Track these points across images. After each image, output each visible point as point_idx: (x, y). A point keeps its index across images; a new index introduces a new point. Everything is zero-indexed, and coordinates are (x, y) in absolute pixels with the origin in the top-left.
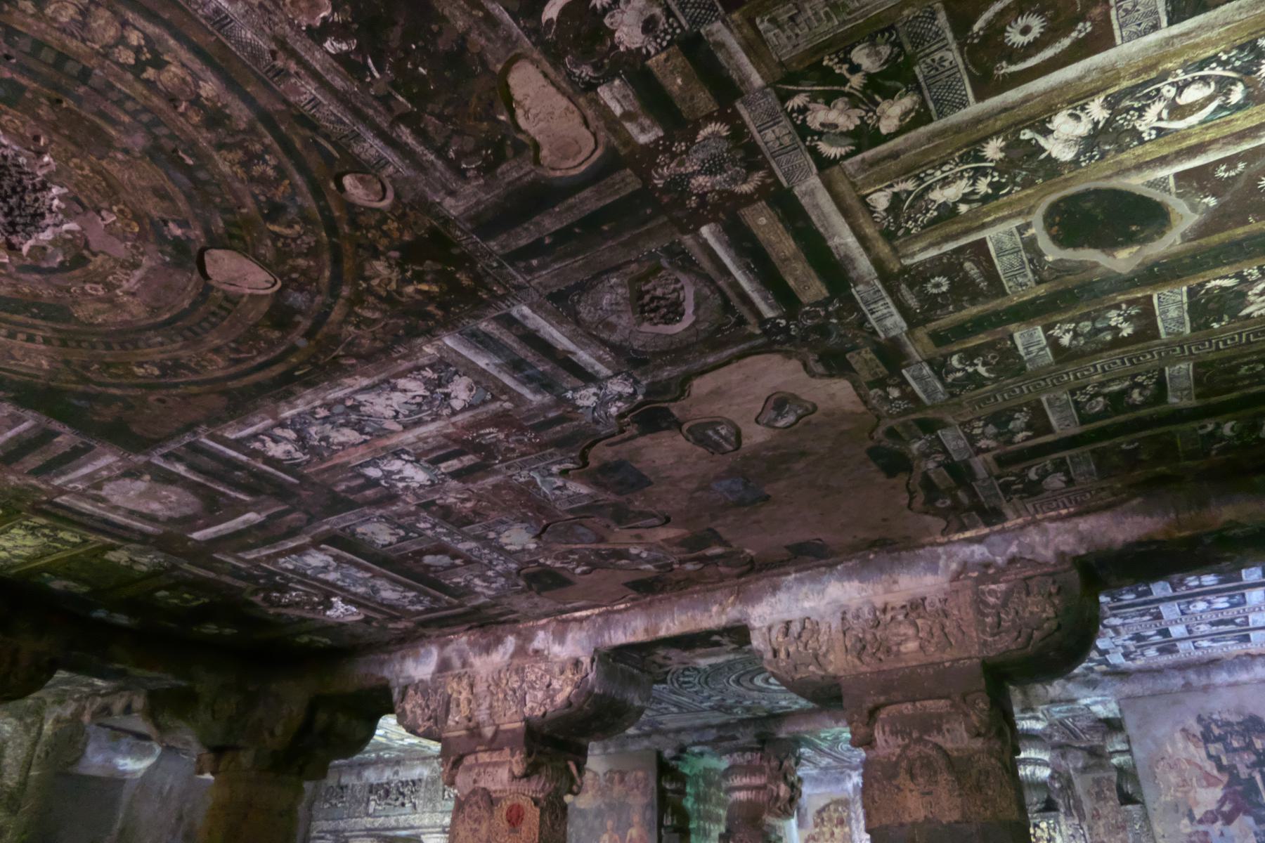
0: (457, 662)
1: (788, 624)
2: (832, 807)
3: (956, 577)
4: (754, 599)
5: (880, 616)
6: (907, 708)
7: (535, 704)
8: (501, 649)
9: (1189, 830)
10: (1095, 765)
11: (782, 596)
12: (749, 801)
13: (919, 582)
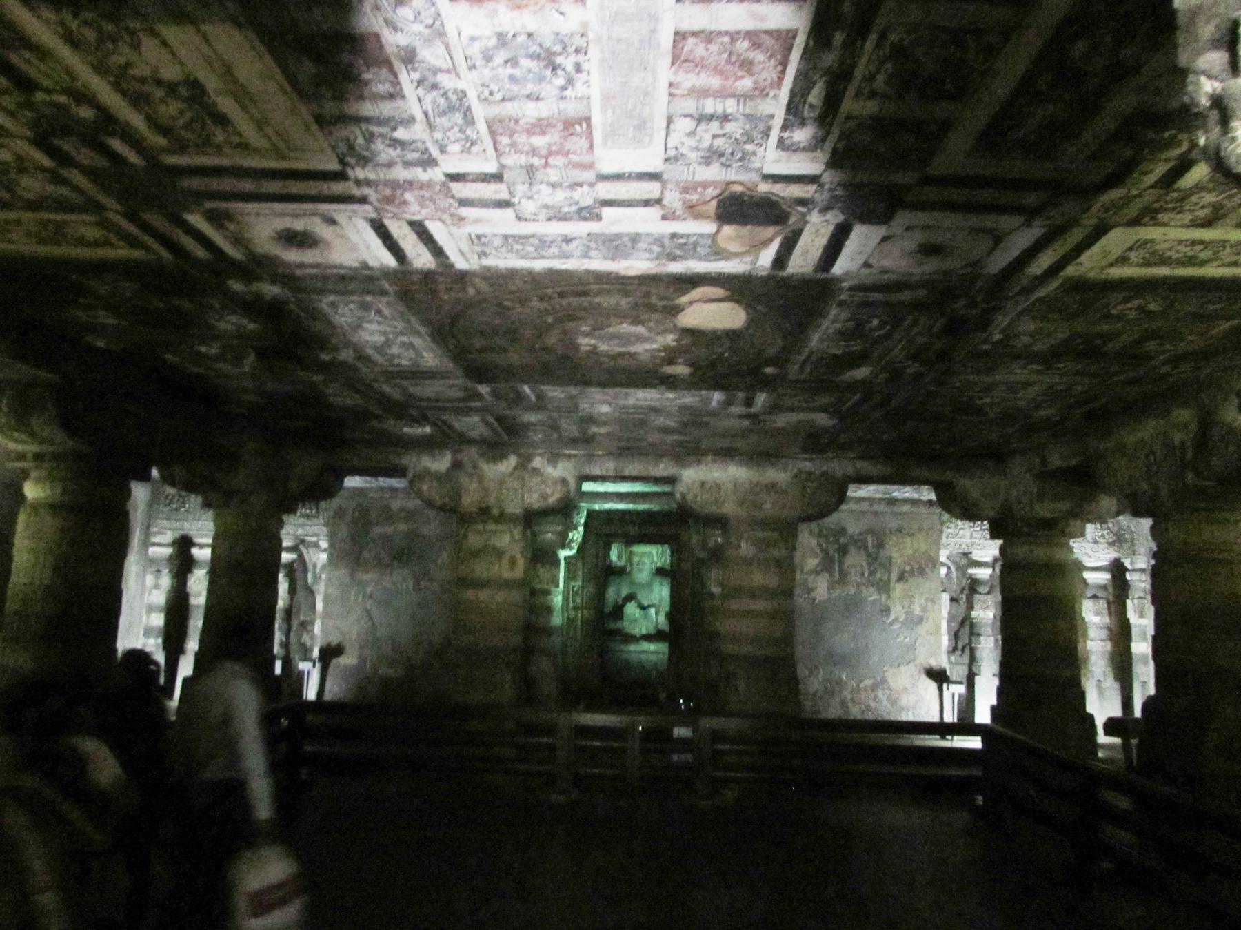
0: (469, 466)
1: (703, 484)
3: (796, 476)
4: (684, 466)
5: (756, 489)
6: (759, 534)
7: (533, 500)
8: (505, 462)
11: (703, 467)
13: (777, 475)
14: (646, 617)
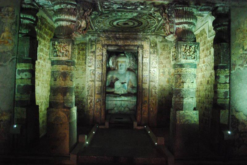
2: (80, 45)
9: (241, 53)
10: (165, 41)
12: (67, 26)
14: (124, 87)
